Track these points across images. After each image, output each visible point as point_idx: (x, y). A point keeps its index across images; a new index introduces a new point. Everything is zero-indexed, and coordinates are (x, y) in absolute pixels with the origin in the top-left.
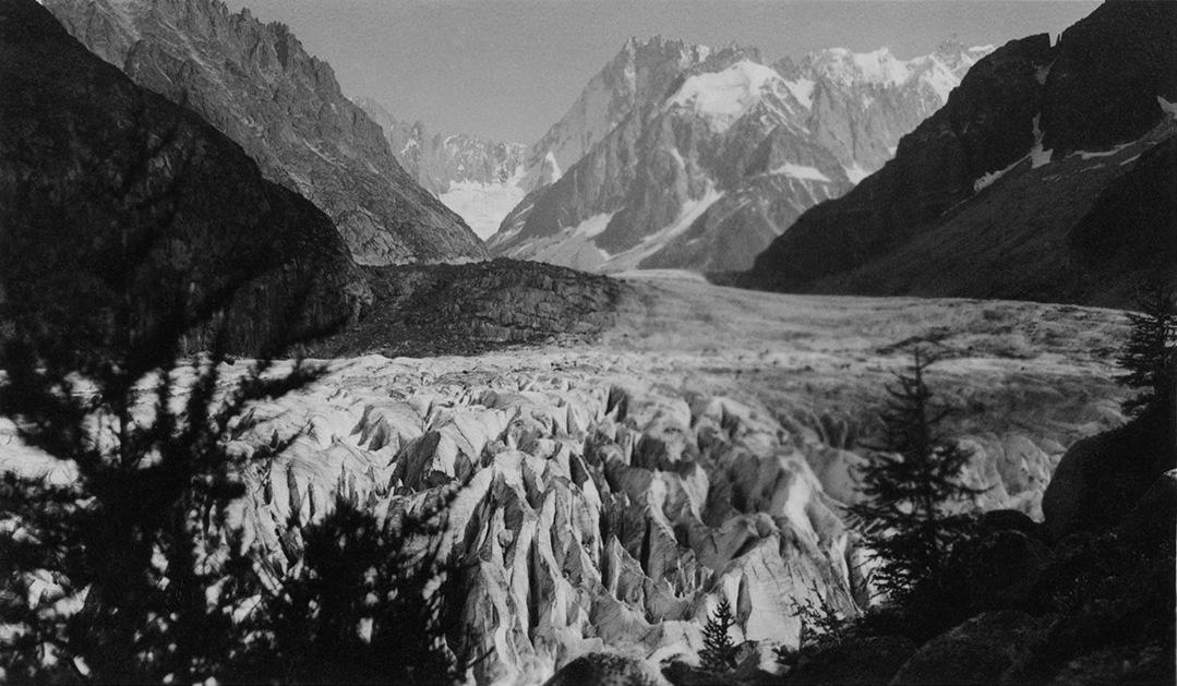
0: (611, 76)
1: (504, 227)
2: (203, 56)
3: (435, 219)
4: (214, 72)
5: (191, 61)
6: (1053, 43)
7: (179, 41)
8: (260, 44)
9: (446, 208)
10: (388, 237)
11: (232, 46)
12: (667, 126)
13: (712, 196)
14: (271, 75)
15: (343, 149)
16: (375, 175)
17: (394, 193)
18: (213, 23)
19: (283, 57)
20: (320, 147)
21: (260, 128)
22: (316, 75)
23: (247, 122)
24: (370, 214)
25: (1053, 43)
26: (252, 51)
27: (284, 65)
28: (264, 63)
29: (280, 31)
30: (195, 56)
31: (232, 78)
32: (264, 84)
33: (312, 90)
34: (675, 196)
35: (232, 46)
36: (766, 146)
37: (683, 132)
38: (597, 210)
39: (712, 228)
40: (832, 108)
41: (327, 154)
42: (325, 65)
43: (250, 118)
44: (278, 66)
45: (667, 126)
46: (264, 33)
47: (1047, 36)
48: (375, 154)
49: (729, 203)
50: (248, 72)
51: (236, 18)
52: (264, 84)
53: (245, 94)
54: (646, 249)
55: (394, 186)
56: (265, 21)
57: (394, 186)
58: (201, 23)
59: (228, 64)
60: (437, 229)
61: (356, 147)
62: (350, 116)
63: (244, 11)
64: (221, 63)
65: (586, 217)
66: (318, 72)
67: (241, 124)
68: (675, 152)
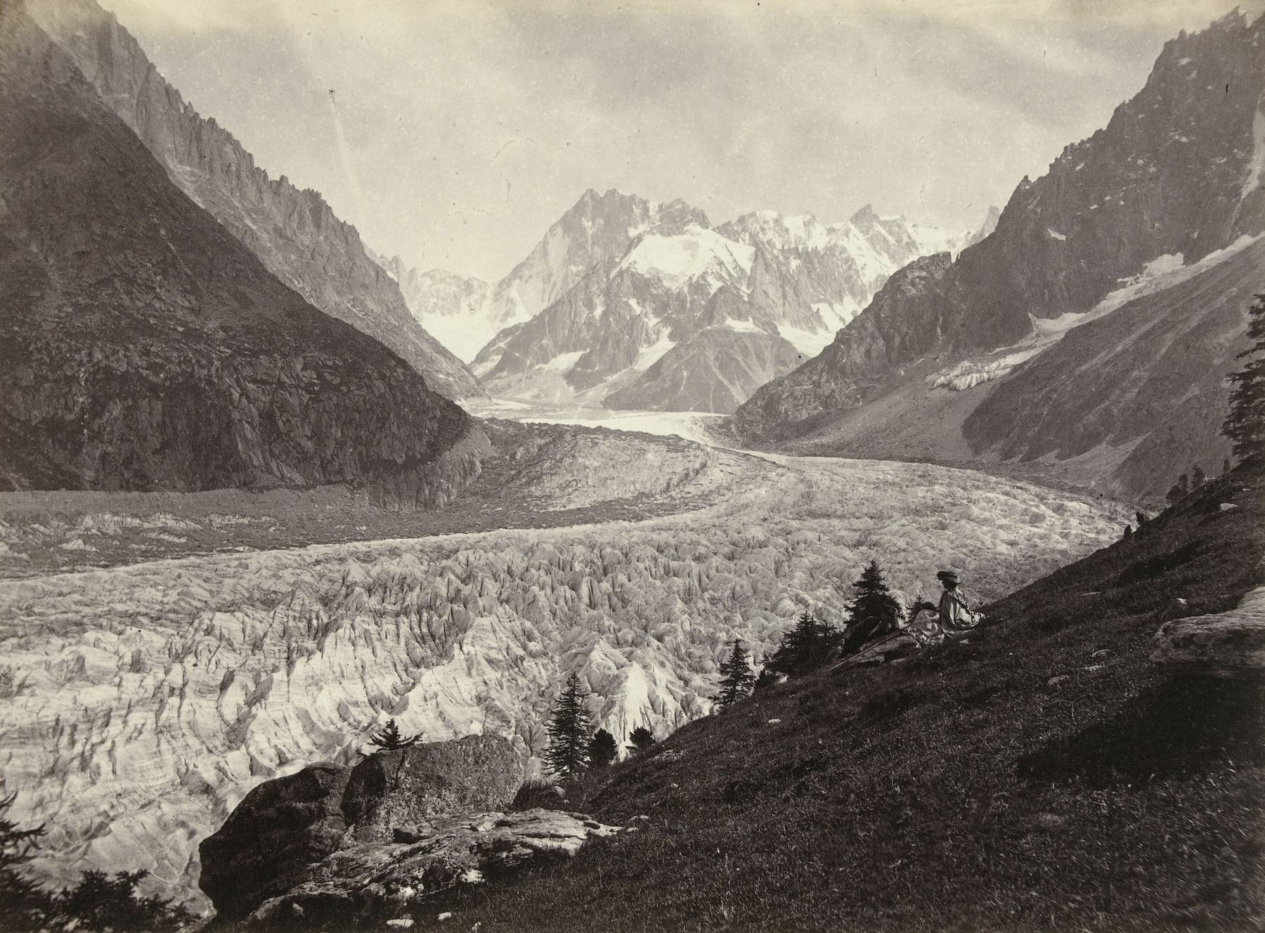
0: (569, 223)
1: (481, 358)
2: (254, 222)
3: (444, 364)
4: (265, 236)
7: (234, 208)
13: (665, 345)
15: (370, 304)
18: (260, 192)
21: (308, 289)
22: (346, 238)
27: (318, 226)
29: (313, 196)
31: (281, 242)
38: (565, 347)
40: (766, 270)
42: (352, 228)
45: (627, 281)
51: (275, 185)
55: (412, 336)
56: (300, 187)
57: (412, 336)
58: (252, 194)
61: (380, 302)
62: (373, 274)
63: (282, 178)
64: (270, 227)
65: (555, 356)
68: (633, 302)
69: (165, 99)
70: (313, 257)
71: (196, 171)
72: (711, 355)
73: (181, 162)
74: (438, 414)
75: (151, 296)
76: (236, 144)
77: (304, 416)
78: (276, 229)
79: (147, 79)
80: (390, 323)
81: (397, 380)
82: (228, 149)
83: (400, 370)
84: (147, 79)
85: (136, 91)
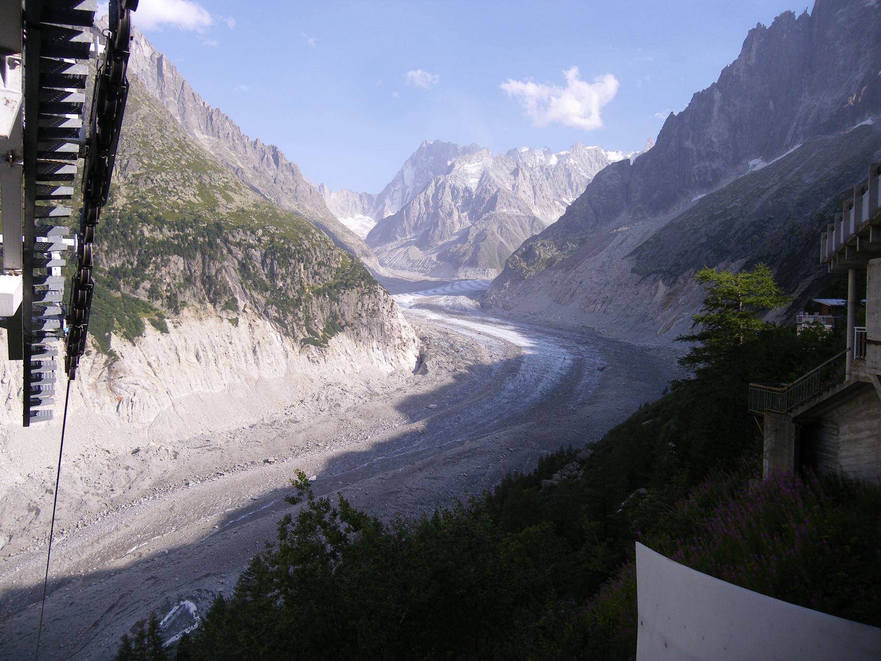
6: (631, 164)
7: (232, 157)
11: (253, 157)
12: (447, 189)
14: (271, 173)
19: (277, 162)
25: (631, 164)
26: (262, 159)
28: (268, 166)
29: (274, 149)
34: (453, 223)
35: (253, 157)
36: (494, 199)
37: (454, 189)
39: (471, 238)
44: (274, 166)
46: (267, 151)
47: (629, 160)
58: (240, 148)
59: (254, 168)
62: (308, 190)
66: (291, 169)
69: (192, 98)
70: (275, 182)
71: (211, 138)
72: (495, 228)
73: (203, 133)
74: (341, 259)
75: (177, 197)
76: (231, 122)
77: (263, 263)
79: (182, 88)
82: (227, 124)
83: (318, 235)
84: (182, 88)
85: (177, 96)
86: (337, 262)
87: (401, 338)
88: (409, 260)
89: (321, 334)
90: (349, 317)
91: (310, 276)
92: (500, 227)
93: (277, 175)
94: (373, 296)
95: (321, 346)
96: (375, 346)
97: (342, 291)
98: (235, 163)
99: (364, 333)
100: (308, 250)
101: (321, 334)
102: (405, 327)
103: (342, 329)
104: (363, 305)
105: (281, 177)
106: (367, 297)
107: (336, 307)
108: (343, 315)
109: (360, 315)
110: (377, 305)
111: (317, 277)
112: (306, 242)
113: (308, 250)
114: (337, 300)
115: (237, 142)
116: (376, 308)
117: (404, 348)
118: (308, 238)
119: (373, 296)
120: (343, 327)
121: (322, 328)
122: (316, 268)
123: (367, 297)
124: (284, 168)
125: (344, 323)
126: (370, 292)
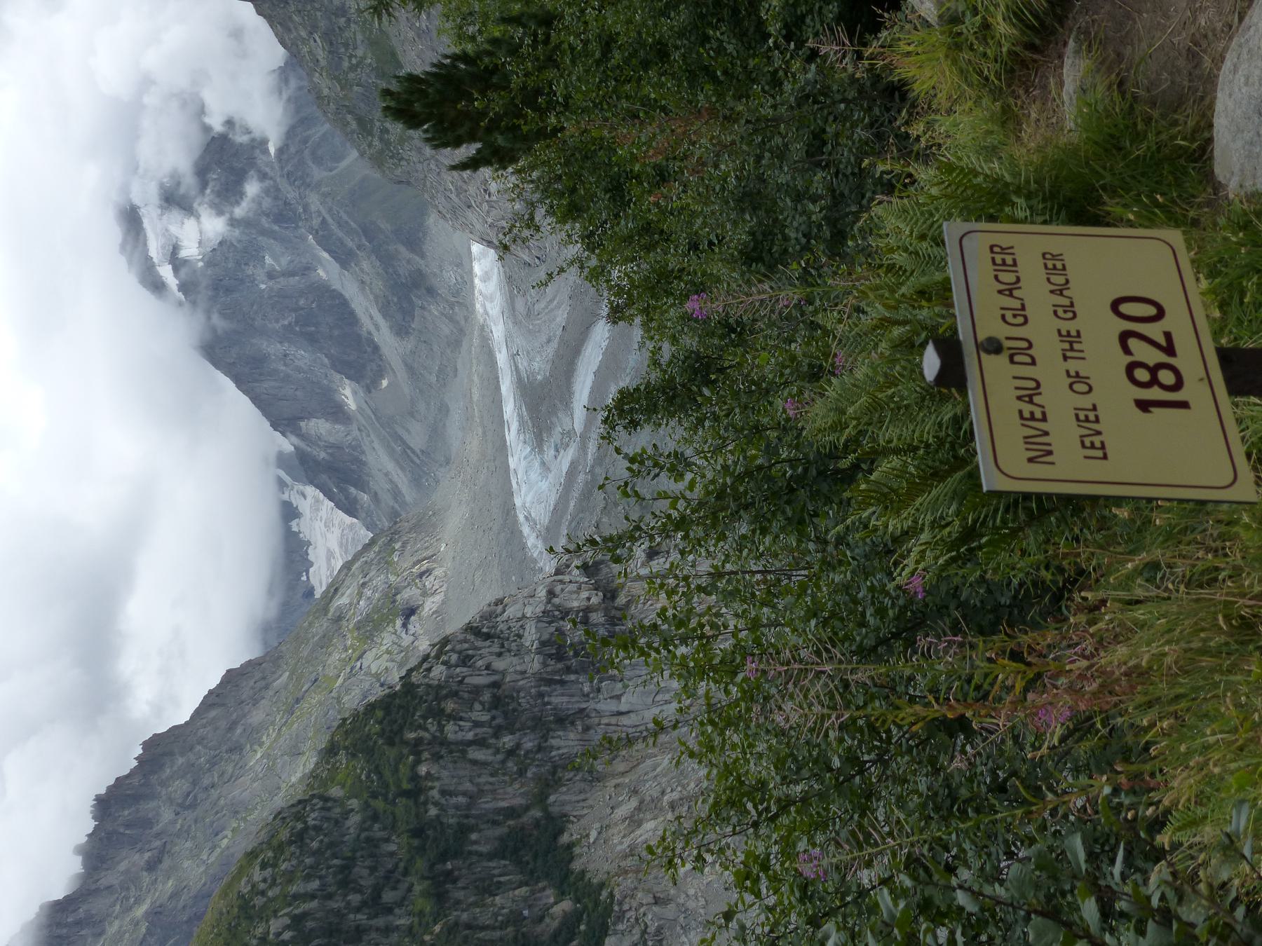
2: (138, 901)
5: (147, 914)
8: (122, 830)
9: (330, 586)
10: (369, 656)
11: (123, 866)
16: (290, 678)
17: (313, 651)
19: (137, 798)
20: (256, 747)
23: (225, 841)
24: (340, 680)
30: (140, 911)
32: (174, 822)
33: (180, 761)
41: (264, 738)
43: (220, 836)
44: (152, 804)
48: (264, 678)
49: (316, 222)
50: (158, 843)
52: (174, 822)
53: (189, 844)
54: (377, 328)
60: (360, 595)
62: (213, 713)
64: (146, 878)
67: (228, 848)
72: (317, 173)
78: (151, 866)
80: (286, 687)
81: (274, 883)
86: (347, 813)
87: (587, 610)
88: (412, 414)
89: (567, 905)
90: (513, 795)
91: (380, 922)
92: (318, 160)
93: (171, 800)
94: (450, 706)
95: (608, 910)
96: (613, 706)
97: (433, 812)
98: (137, 924)
99: (566, 742)
100: (297, 920)
101: (567, 905)
102: (551, 594)
103: (555, 824)
104: (480, 743)
105: (180, 787)
106: (450, 728)
107: (483, 840)
108: (512, 813)
109: (511, 753)
110: (477, 690)
111: (388, 896)
112: (275, 925)
113: (297, 920)
114: (463, 831)
115: (81, 913)
116: (486, 697)
117: (621, 600)
118: (263, 915)
119: (450, 706)
120: (549, 817)
121: (549, 896)
122: (355, 898)
123: (450, 728)
124: (154, 779)
125: (537, 813)
126: (438, 714)
